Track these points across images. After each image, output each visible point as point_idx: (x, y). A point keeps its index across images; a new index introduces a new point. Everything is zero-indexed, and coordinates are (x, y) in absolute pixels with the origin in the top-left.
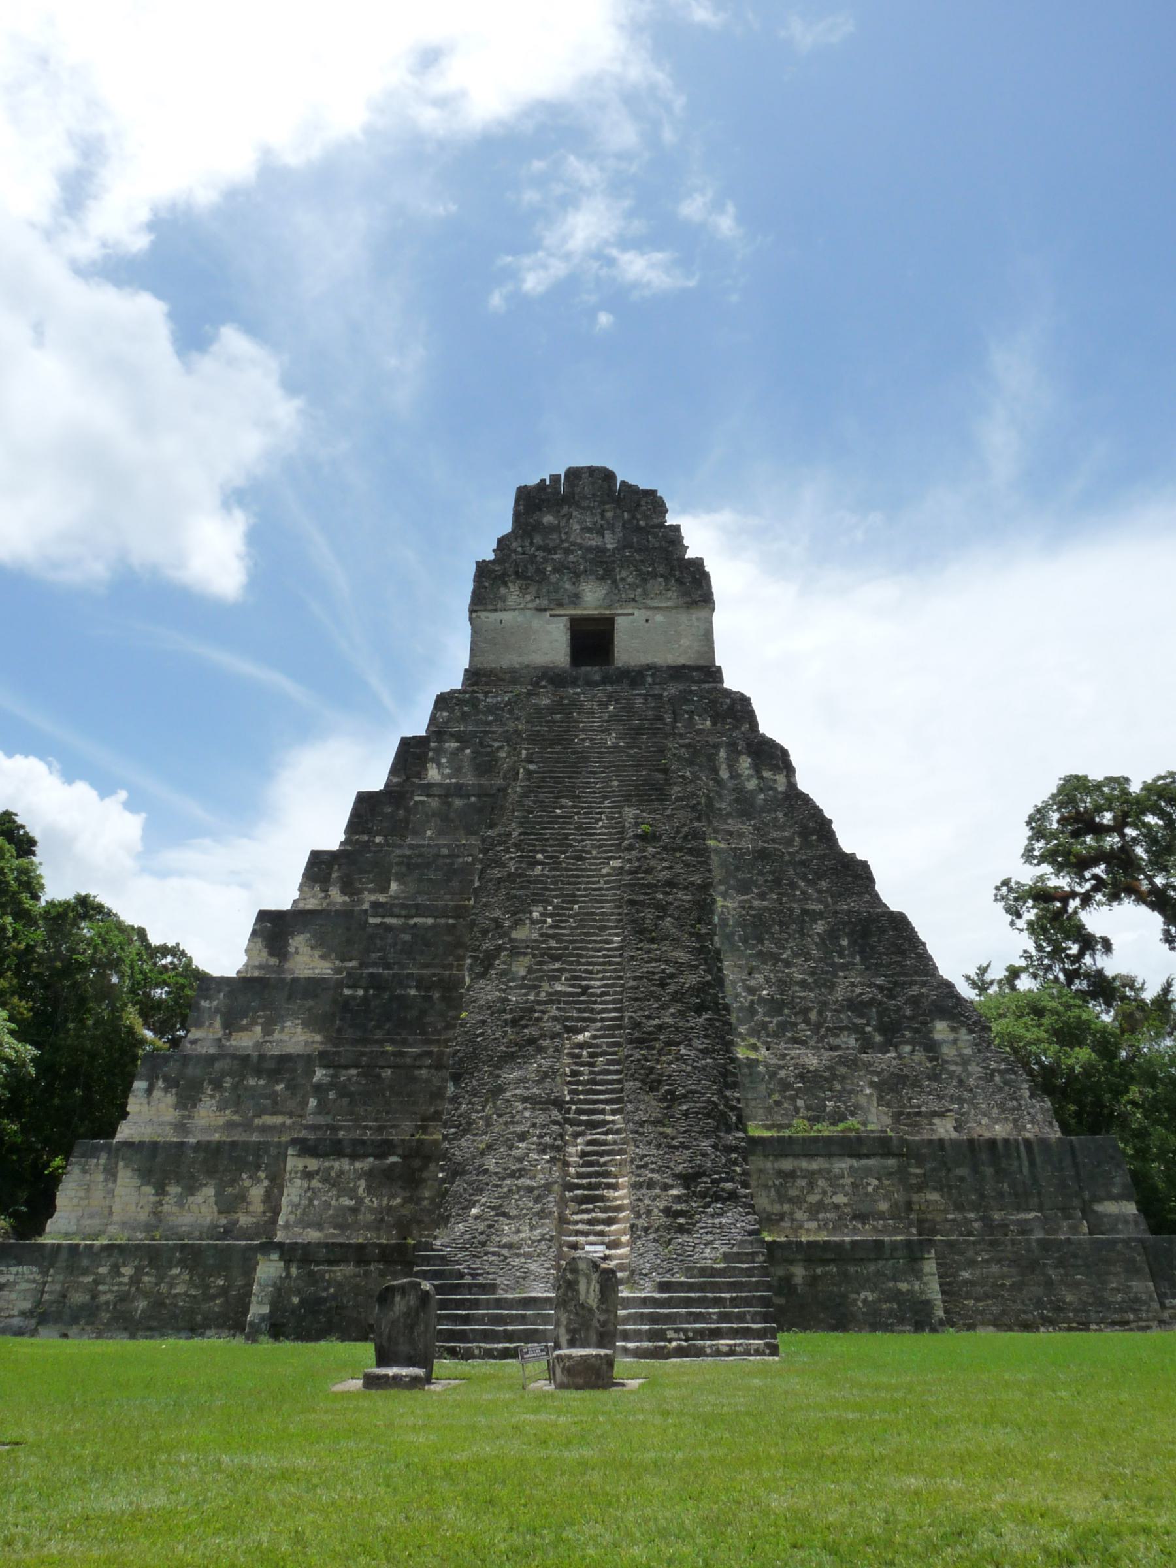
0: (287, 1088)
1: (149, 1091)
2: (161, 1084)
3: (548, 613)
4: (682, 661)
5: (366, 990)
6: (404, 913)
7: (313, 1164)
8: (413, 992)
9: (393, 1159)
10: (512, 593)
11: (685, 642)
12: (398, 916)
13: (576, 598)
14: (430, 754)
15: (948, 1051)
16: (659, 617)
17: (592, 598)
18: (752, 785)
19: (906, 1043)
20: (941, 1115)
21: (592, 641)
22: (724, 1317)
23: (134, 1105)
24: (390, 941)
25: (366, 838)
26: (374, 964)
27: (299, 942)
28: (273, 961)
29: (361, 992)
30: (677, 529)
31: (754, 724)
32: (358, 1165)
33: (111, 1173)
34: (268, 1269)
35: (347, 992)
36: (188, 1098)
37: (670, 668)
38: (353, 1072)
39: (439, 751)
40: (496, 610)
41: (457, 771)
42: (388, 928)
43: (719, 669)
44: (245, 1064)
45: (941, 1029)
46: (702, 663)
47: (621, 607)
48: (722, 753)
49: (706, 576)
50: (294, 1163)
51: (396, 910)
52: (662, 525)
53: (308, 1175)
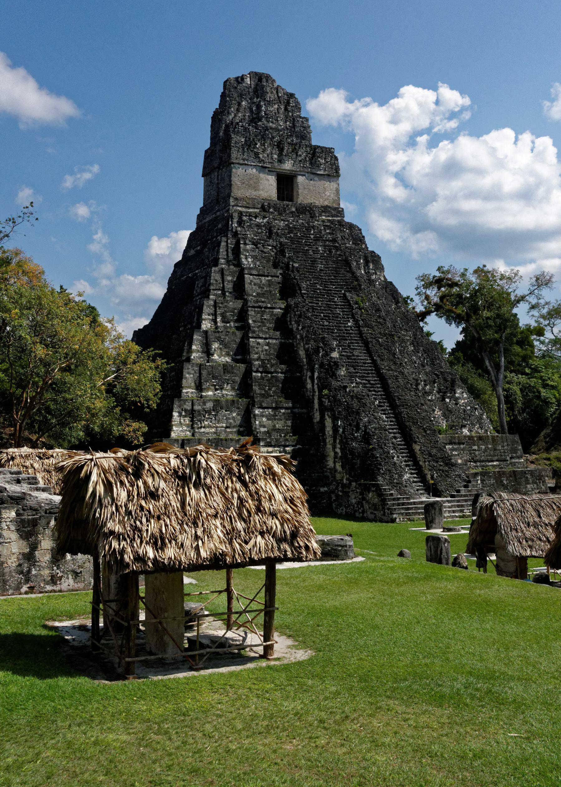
0: (238, 415)
1: (180, 415)
3: (267, 170)
4: (326, 203)
5: (261, 373)
6: (264, 336)
11: (327, 193)
12: (262, 338)
13: (280, 161)
19: (448, 397)
24: (260, 349)
26: (257, 360)
27: (215, 345)
28: (204, 355)
29: (259, 375)
30: (307, 120)
35: (254, 374)
37: (322, 207)
38: (270, 410)
40: (242, 164)
42: (258, 344)
46: (335, 206)
47: (300, 171)
48: (362, 261)
51: (261, 335)
52: (301, 117)
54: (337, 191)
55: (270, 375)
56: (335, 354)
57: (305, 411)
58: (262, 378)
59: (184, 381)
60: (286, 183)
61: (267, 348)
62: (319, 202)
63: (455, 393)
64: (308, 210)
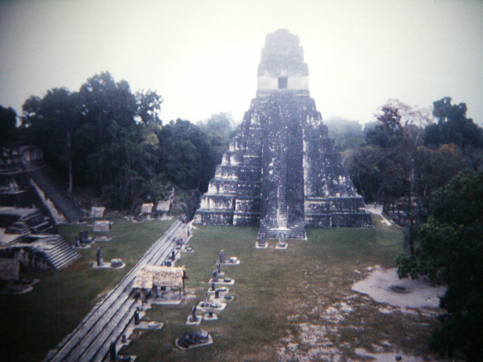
0: (234, 186)
1: (212, 186)
2: (213, 185)
7: (240, 201)
8: (252, 171)
9: (252, 201)
10: (266, 72)
13: (279, 73)
14: (252, 117)
15: (341, 182)
16: (297, 78)
17: (283, 73)
18: (313, 124)
20: (337, 193)
21: (283, 82)
22: (298, 233)
23: (209, 189)
25: (240, 135)
28: (227, 162)
31: (315, 106)
32: (247, 201)
33: (208, 200)
34: (235, 217)
36: (218, 188)
37: (299, 90)
38: (244, 185)
39: (253, 116)
41: (257, 120)
42: (247, 158)
43: (309, 91)
44: (226, 182)
45: (340, 178)
46: (306, 89)
48: (308, 117)
49: (308, 68)
50: (237, 201)
53: (239, 203)
54: (307, 83)
55: (248, 171)
56: (271, 165)
57: (259, 186)
58: (245, 172)
59: (216, 173)
60: (283, 82)
61: (250, 159)
62: (298, 88)
63: (339, 177)
64: (290, 94)
